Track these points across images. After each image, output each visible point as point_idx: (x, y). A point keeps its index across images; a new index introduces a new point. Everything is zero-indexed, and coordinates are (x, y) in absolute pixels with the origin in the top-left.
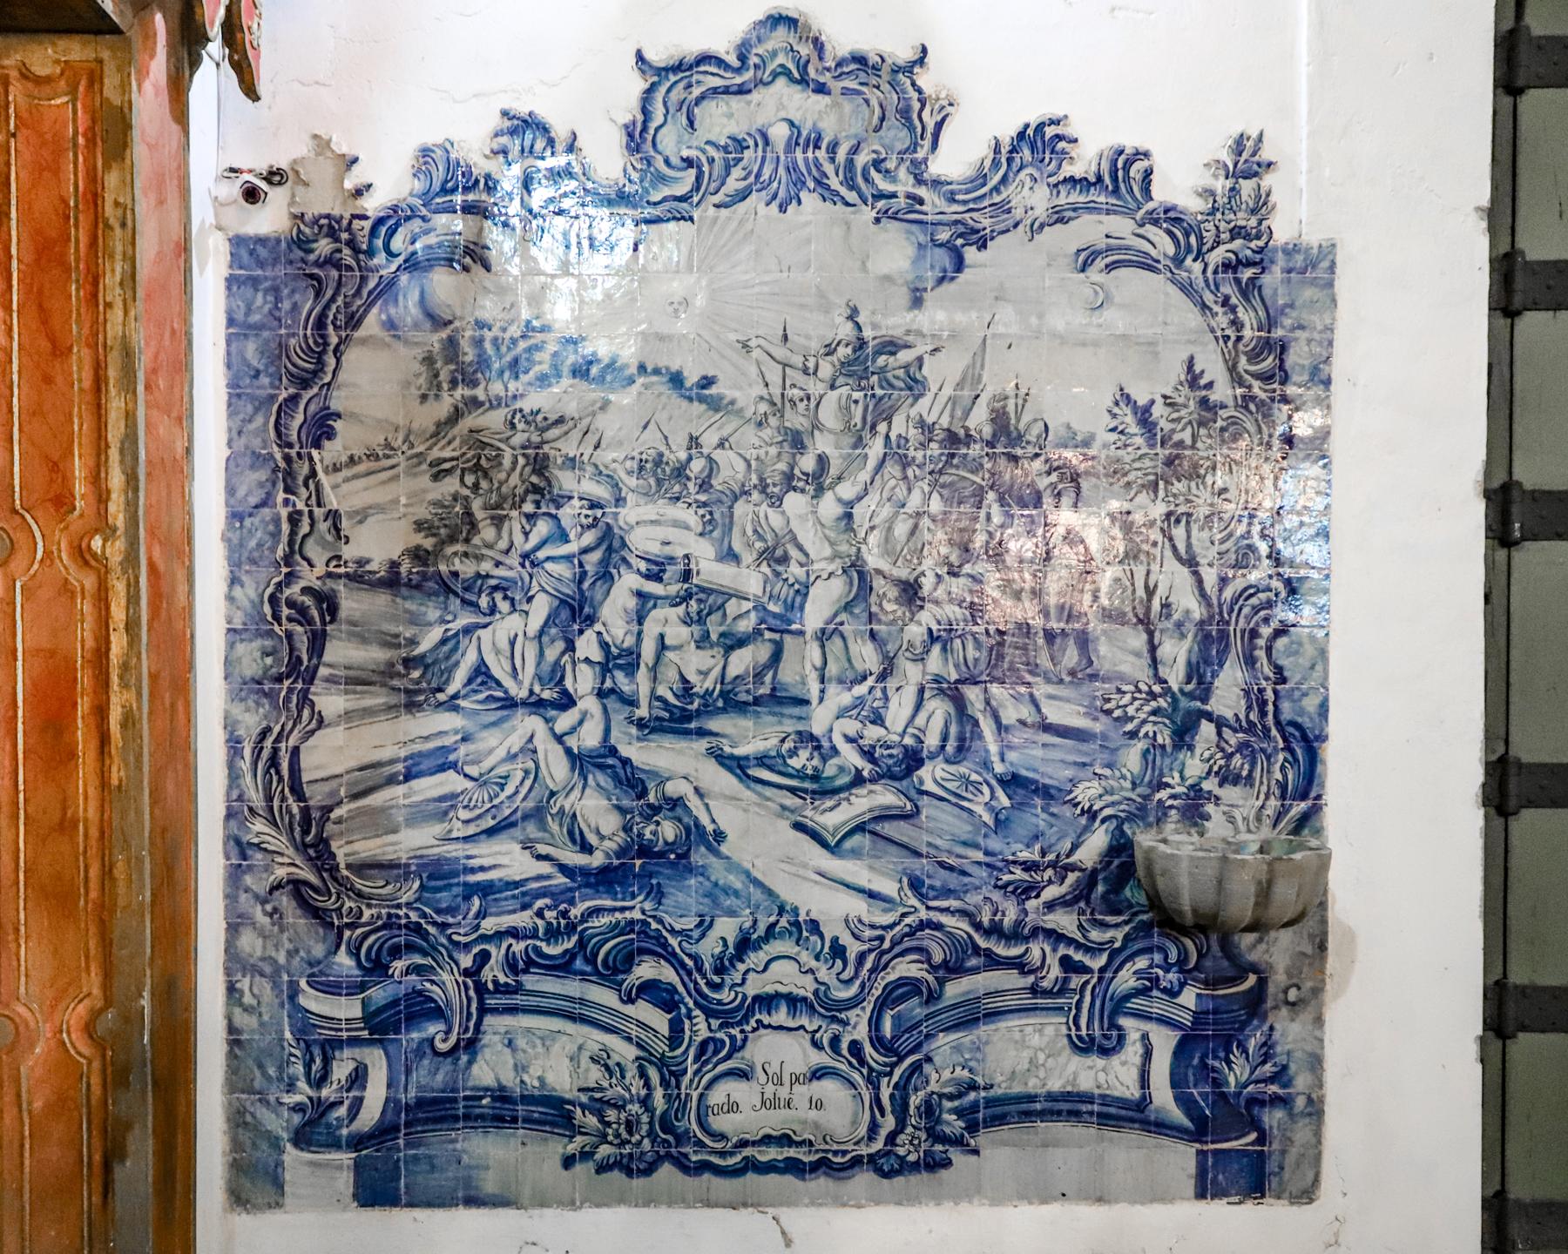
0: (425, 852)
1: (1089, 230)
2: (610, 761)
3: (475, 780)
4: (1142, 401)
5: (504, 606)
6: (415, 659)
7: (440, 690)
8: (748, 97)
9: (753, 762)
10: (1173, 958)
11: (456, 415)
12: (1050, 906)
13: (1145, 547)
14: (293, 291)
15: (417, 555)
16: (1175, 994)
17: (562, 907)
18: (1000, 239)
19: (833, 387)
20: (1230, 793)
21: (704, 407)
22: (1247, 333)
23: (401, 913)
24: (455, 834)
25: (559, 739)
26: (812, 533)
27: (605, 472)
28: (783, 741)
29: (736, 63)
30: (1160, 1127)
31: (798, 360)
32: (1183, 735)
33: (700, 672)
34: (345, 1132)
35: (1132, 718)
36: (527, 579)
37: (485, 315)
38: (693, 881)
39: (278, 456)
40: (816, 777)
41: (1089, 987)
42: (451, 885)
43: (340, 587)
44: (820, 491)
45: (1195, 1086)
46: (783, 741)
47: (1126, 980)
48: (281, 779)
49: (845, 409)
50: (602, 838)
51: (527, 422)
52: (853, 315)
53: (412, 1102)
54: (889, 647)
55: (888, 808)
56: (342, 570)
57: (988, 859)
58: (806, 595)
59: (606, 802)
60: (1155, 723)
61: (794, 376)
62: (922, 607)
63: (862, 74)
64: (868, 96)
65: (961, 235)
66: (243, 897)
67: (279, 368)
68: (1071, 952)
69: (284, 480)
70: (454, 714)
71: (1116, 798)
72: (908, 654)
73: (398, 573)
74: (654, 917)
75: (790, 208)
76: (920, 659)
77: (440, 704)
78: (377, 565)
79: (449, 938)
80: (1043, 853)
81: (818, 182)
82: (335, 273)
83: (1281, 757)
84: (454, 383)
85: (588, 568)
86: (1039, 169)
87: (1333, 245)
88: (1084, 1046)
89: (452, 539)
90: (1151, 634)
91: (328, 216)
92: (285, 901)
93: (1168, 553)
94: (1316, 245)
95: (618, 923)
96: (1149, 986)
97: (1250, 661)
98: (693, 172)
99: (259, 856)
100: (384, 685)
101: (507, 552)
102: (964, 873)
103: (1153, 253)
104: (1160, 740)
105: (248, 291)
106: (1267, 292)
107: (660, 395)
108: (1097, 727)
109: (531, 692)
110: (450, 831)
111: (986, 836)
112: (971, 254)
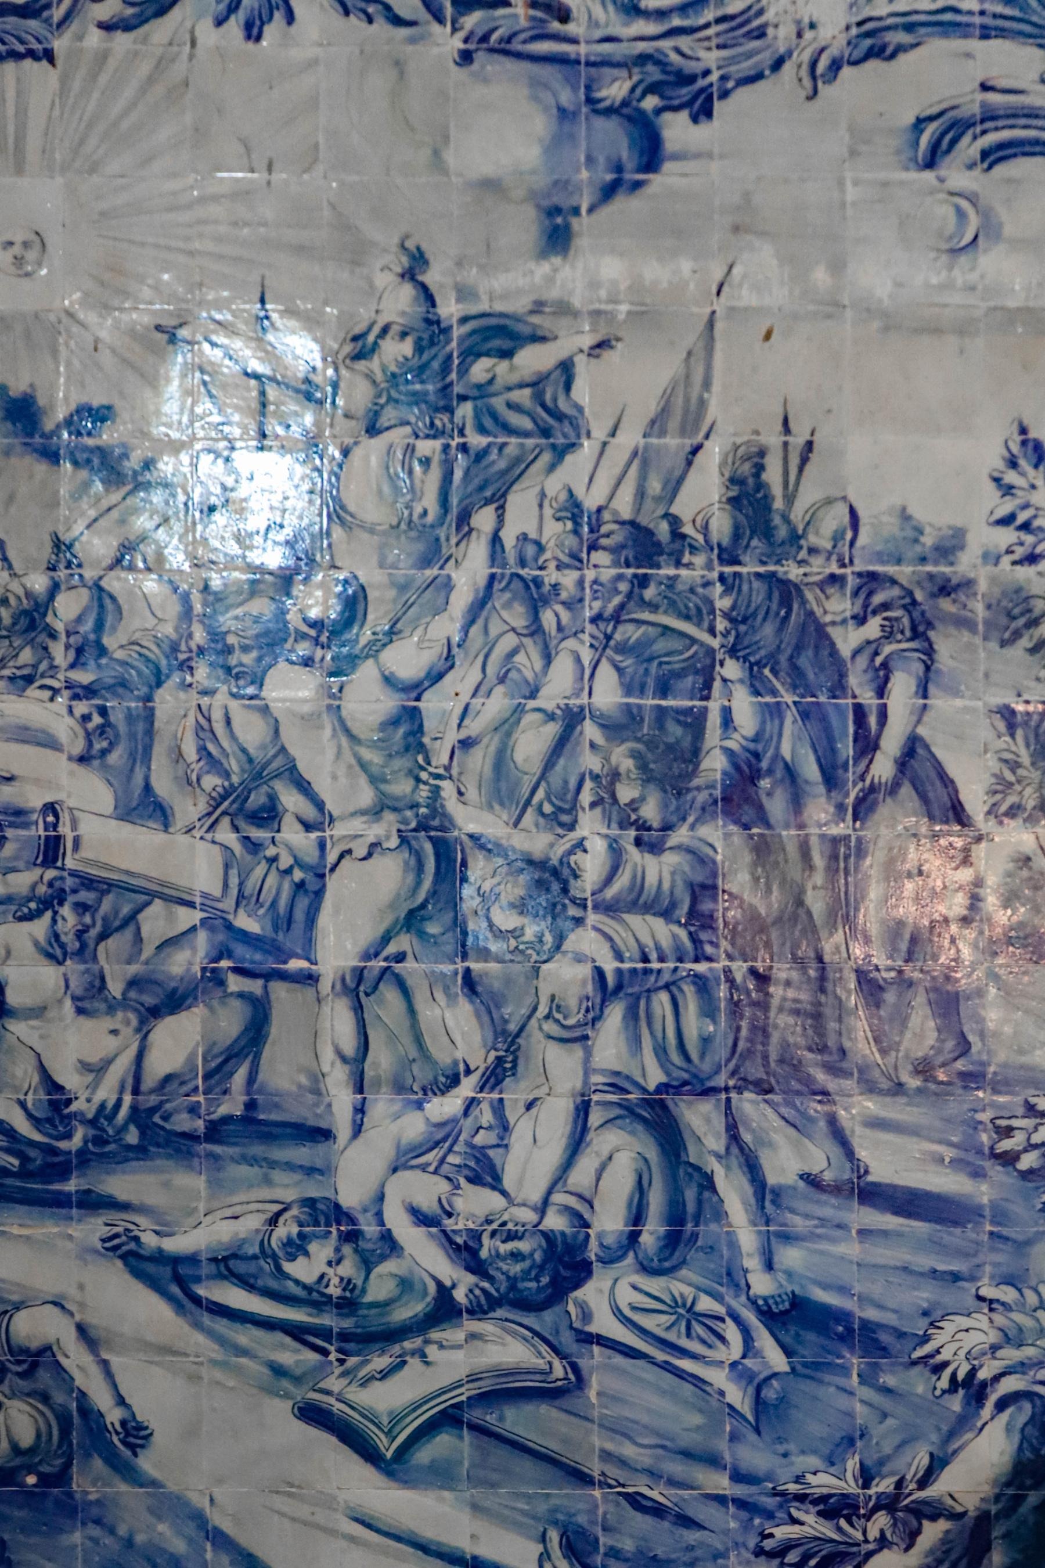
9: (206, 1269)
18: (743, 96)
19: (373, 430)
26: (330, 753)
28: (273, 1221)
33: (85, 1067)
38: (77, 1537)
46: (273, 1221)
54: (506, 1011)
57: (740, 1491)
58: (319, 894)
62: (579, 921)
65: (653, 89)
72: (550, 1027)
80: (866, 1477)
102: (686, 1521)
108: (983, 1193)
111: (734, 1437)
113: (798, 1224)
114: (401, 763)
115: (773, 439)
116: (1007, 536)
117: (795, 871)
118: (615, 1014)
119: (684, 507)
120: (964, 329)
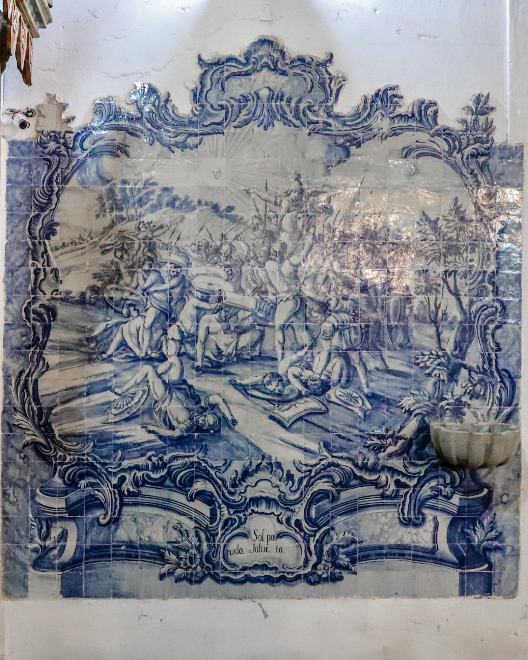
0: (96, 429)
2: (183, 386)
3: (119, 395)
5: (134, 313)
6: (92, 338)
7: (104, 353)
8: (250, 77)
9: (250, 387)
10: (448, 481)
11: (113, 224)
12: (390, 456)
13: (435, 286)
14: (38, 166)
15: (94, 289)
17: (160, 455)
18: (367, 143)
19: (289, 211)
20: (475, 403)
21: (228, 220)
23: (84, 458)
24: (110, 421)
25: (159, 376)
26: (279, 279)
27: (182, 251)
29: (244, 61)
30: (442, 561)
31: (272, 199)
32: (453, 375)
33: (226, 345)
34: (57, 562)
35: (428, 367)
36: (145, 301)
37: (126, 177)
39: (30, 243)
40: (279, 395)
41: (409, 495)
42: (108, 445)
43: (58, 304)
44: (282, 260)
45: (459, 542)
46: (264, 377)
47: (426, 491)
48: (29, 395)
49: (294, 223)
50: (179, 423)
51: (146, 228)
52: (298, 178)
53: (88, 548)
55: (314, 409)
56: (59, 296)
57: (361, 434)
58: (276, 309)
59: (181, 406)
60: (440, 369)
61: (270, 206)
62: (330, 315)
63: (303, 67)
64: (306, 76)
65: (348, 141)
66: (10, 450)
67: (31, 202)
69: (32, 254)
70: (110, 364)
71: (421, 405)
72: (323, 337)
73: (85, 298)
74: (203, 460)
75: (269, 129)
76: (329, 339)
77: (104, 359)
78: (75, 294)
79: (107, 470)
80: (387, 431)
81: (282, 116)
82: (57, 158)
83: (499, 386)
84: (112, 209)
85: (173, 295)
86: (385, 110)
87: (522, 146)
88: (406, 523)
89: (111, 282)
91: (54, 132)
92: (29, 451)
93: (446, 289)
94: (514, 146)
95: (186, 463)
96: (437, 494)
97: (485, 341)
98: (224, 111)
99: (18, 430)
100: (78, 350)
101: (136, 288)
102: (349, 440)
103: (438, 149)
104: (442, 377)
105: (17, 167)
106: (491, 167)
107: (208, 214)
108: (412, 371)
109: (147, 354)
110: (108, 419)
111: (360, 422)
112: (353, 149)
113: (374, 377)
114: (294, 281)
118: (337, 334)
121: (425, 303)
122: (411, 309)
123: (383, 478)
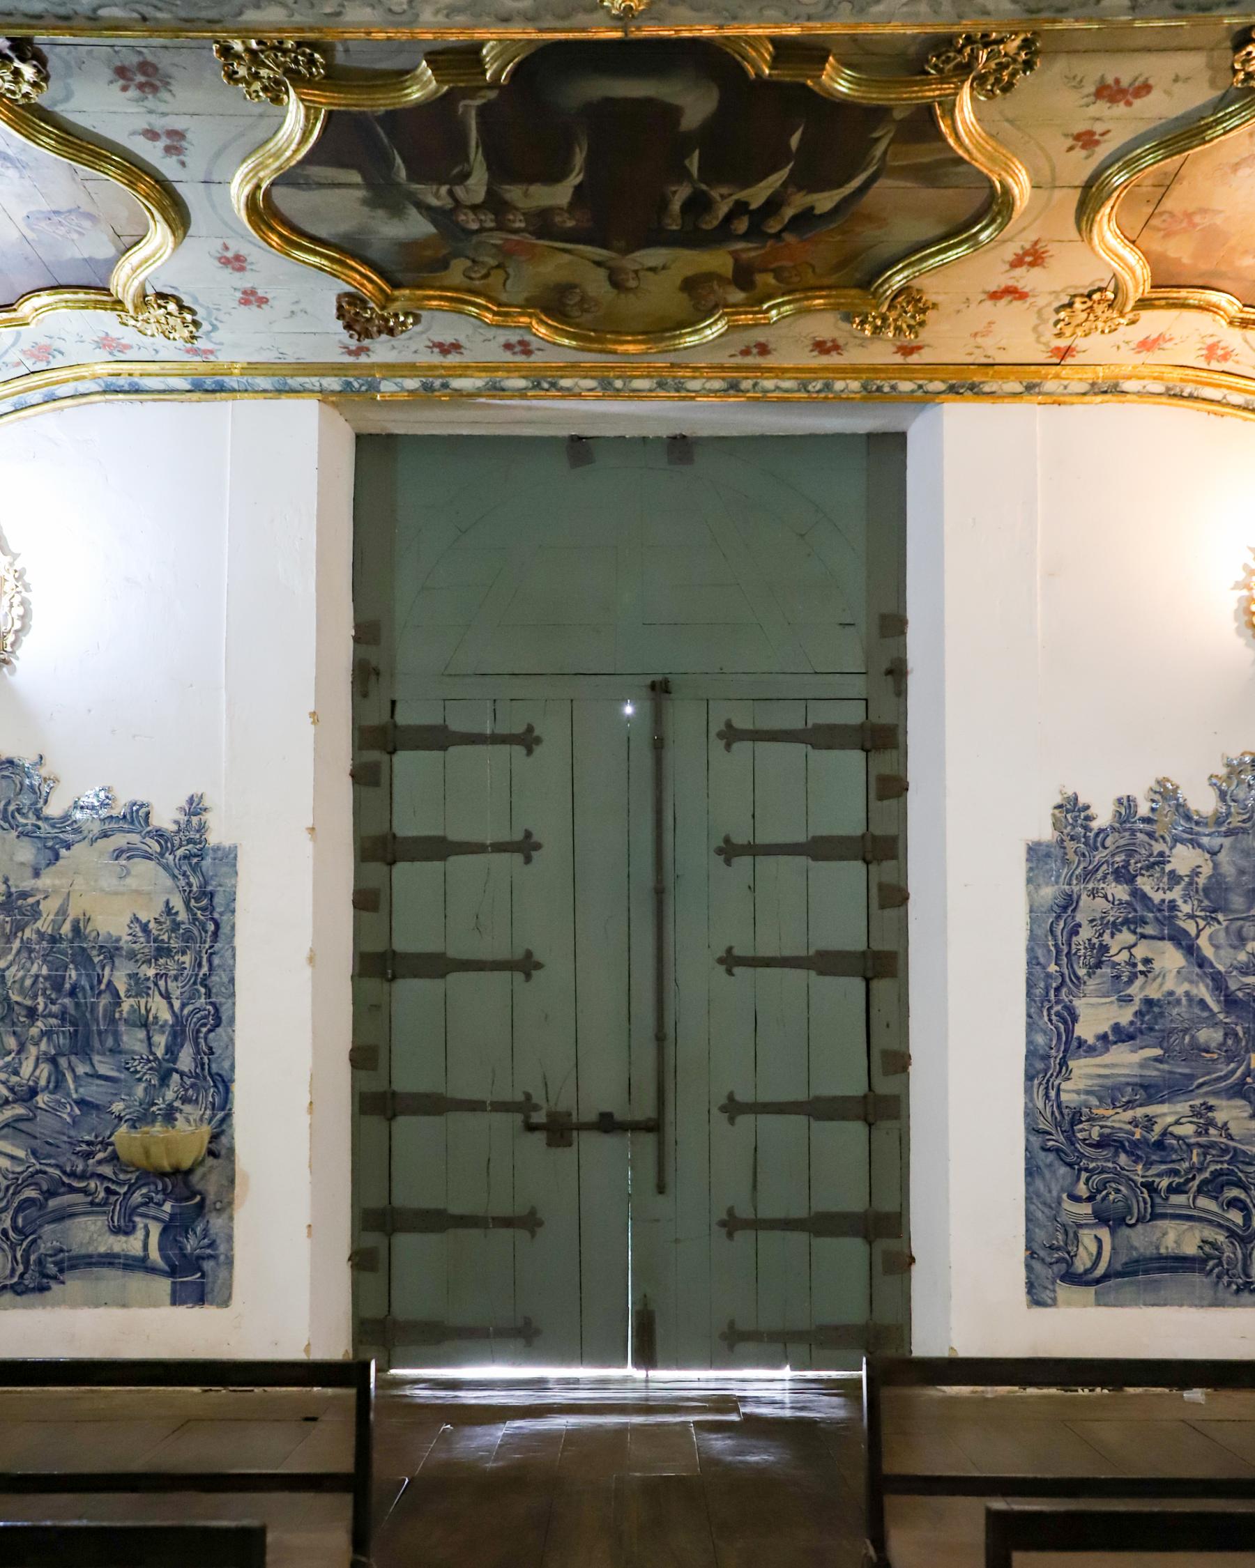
1: (120, 840)
4: (144, 921)
10: (160, 1188)
12: (100, 1162)
16: (161, 1205)
20: (187, 1108)
22: (195, 889)
30: (153, 1270)
32: (164, 1079)
35: (139, 1072)
45: (171, 1249)
47: (137, 1197)
52: (6, 881)
55: (22, 1115)
68: (110, 1185)
76: (37, 1044)
80: (96, 1137)
83: (212, 1090)
88: (116, 1231)
90: (148, 1032)
93: (157, 993)
94: (227, 846)
96: (149, 1201)
97: (197, 1044)
102: (58, 1147)
103: (150, 851)
104: (153, 1082)
106: (204, 869)
108: (122, 1076)
112: (63, 852)
113: (84, 1084)
115: (82, 917)
116: (130, 938)
117: (84, 1008)
118: (45, 1039)
119: (63, 931)
120: (122, 894)
121: (136, 1007)
122: (121, 1012)
123: (92, 1185)
